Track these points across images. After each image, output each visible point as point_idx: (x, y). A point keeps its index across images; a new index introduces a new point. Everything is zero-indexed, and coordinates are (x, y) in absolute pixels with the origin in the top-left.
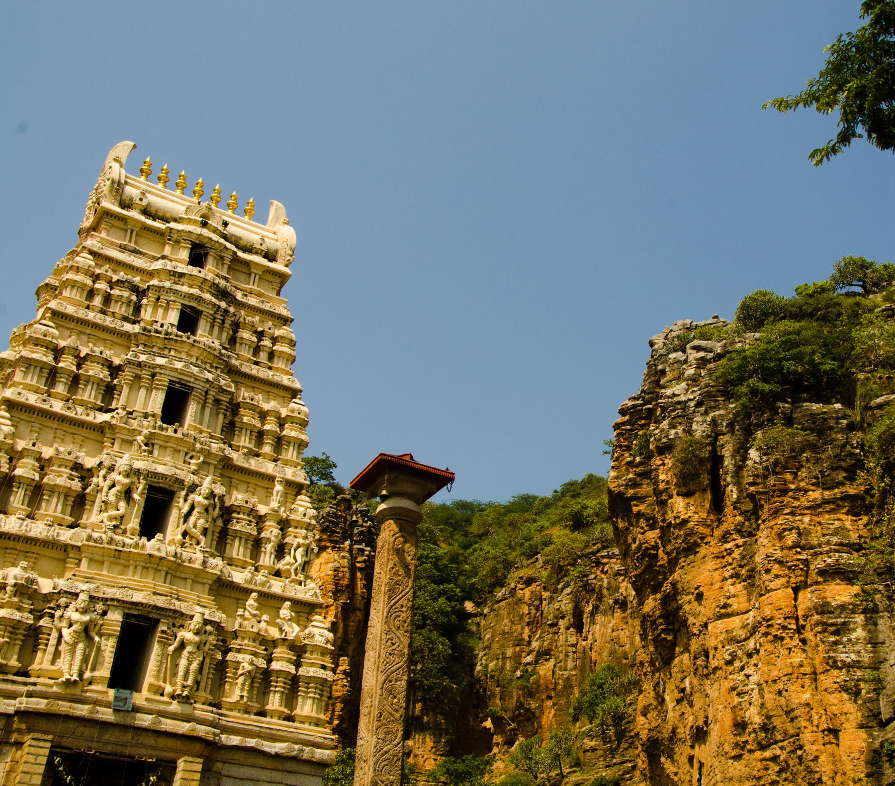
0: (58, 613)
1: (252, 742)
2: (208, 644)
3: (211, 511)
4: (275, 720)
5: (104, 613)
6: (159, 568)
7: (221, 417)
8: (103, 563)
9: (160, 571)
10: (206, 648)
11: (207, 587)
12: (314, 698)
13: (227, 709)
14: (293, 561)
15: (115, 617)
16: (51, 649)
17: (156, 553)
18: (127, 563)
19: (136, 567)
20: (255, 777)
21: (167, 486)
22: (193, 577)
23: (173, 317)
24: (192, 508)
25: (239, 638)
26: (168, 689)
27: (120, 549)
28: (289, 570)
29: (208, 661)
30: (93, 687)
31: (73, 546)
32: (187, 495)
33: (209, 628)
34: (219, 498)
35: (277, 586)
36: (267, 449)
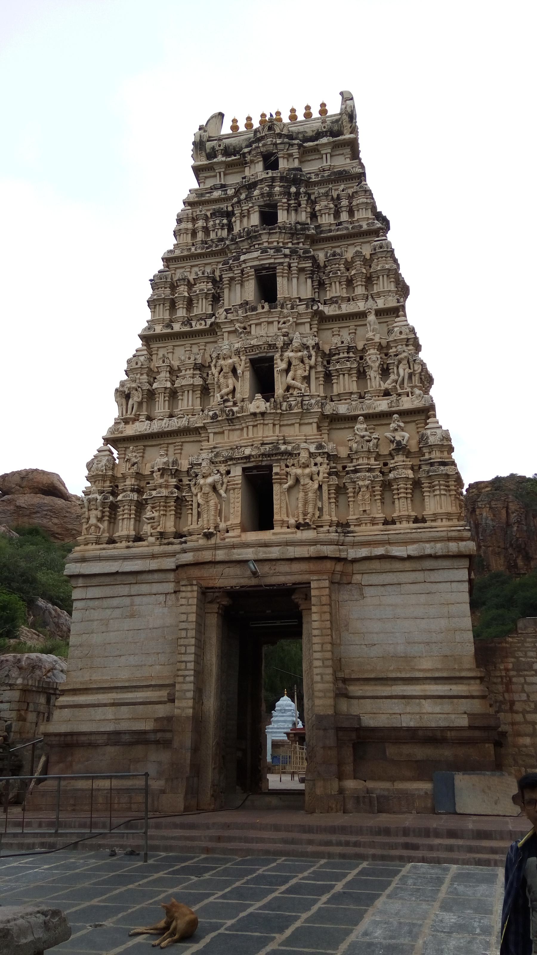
0: (192, 483)
1: (380, 551)
2: (321, 474)
3: (306, 360)
4: (405, 525)
5: (228, 472)
6: (266, 422)
7: (309, 281)
8: (223, 433)
9: (267, 424)
10: (321, 477)
11: (315, 425)
12: (440, 495)
13: (355, 525)
14: (396, 377)
15: (237, 471)
16: (195, 512)
17: (258, 411)
18: (241, 427)
19: (247, 427)
20: (395, 581)
21: (264, 355)
22: (298, 421)
23: (255, 219)
24: (290, 364)
25: (355, 461)
26: (292, 521)
27: (230, 417)
28: (395, 386)
29: (325, 488)
30: (230, 534)
31: (201, 427)
32: (282, 355)
33: (319, 459)
34: (313, 347)
35: (383, 405)
36: (360, 290)
